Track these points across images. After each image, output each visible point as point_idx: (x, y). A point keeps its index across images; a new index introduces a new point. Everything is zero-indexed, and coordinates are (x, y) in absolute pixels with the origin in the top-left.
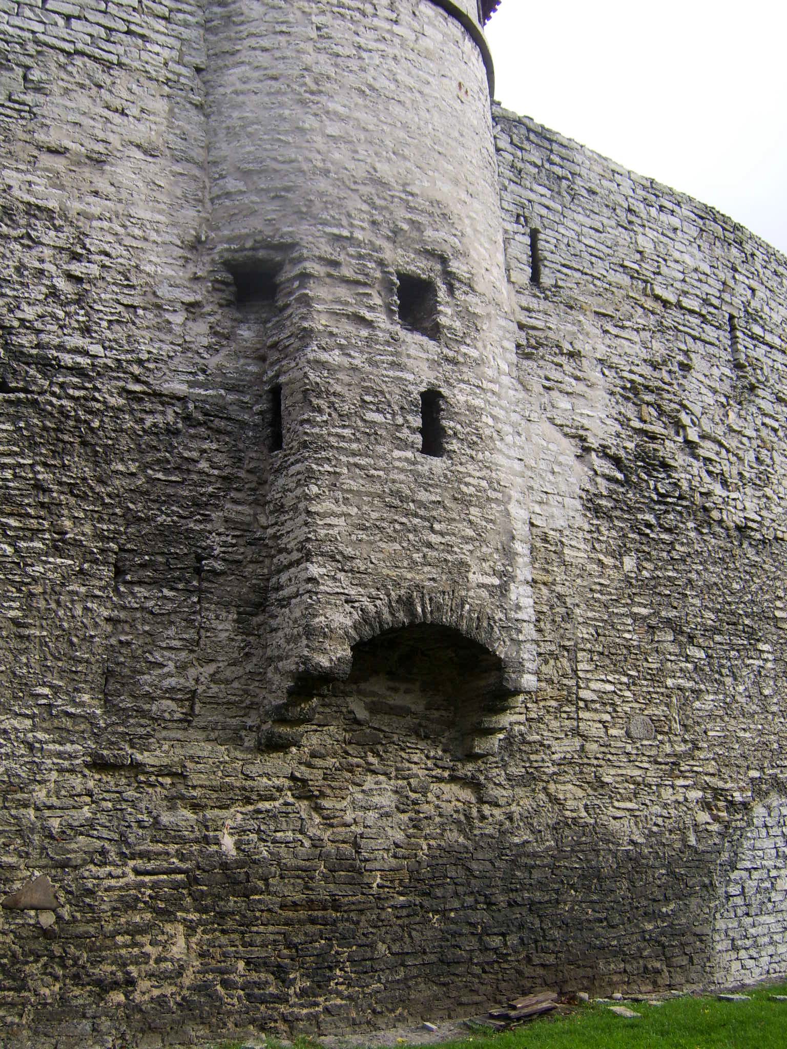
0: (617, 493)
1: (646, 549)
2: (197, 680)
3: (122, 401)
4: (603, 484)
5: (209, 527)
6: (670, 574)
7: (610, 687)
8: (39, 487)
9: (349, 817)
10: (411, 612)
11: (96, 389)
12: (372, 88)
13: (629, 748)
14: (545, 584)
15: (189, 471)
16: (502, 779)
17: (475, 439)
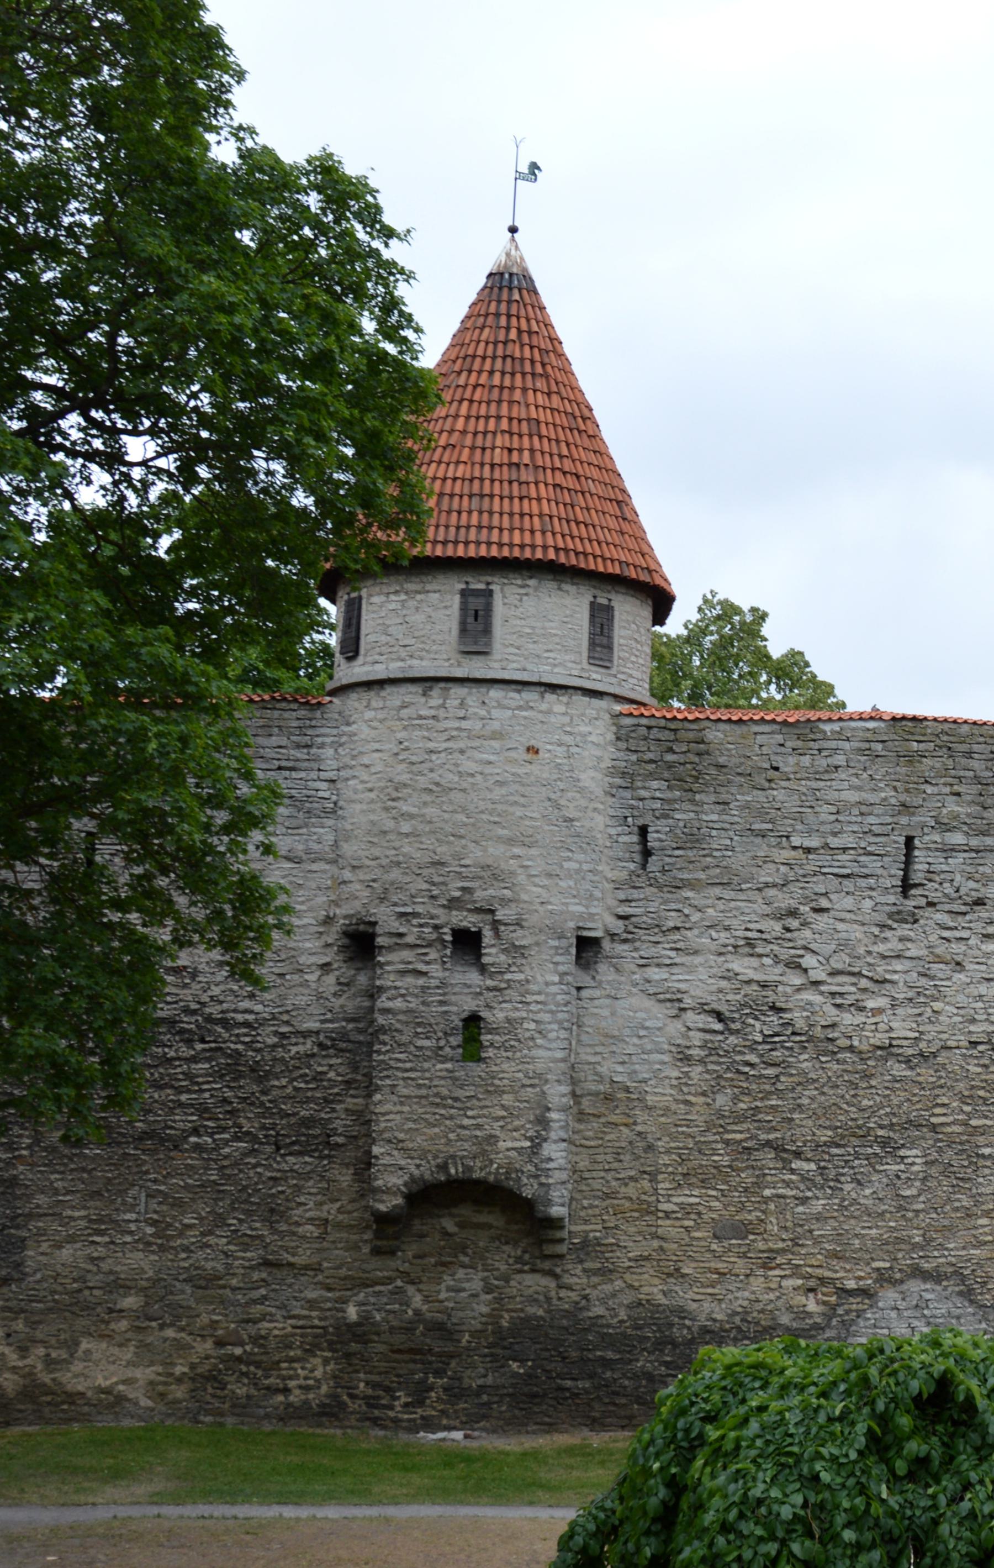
0: (712, 1041)
1: (745, 1085)
2: (329, 1212)
3: (276, 1040)
4: (697, 1038)
5: (335, 1115)
6: (773, 1102)
7: (697, 1200)
8: (225, 1101)
9: (443, 1295)
10: (449, 1174)
11: (258, 1034)
12: (437, 784)
13: (714, 1247)
14: (626, 1125)
15: (322, 1080)
16: (578, 1271)
17: (512, 1043)
